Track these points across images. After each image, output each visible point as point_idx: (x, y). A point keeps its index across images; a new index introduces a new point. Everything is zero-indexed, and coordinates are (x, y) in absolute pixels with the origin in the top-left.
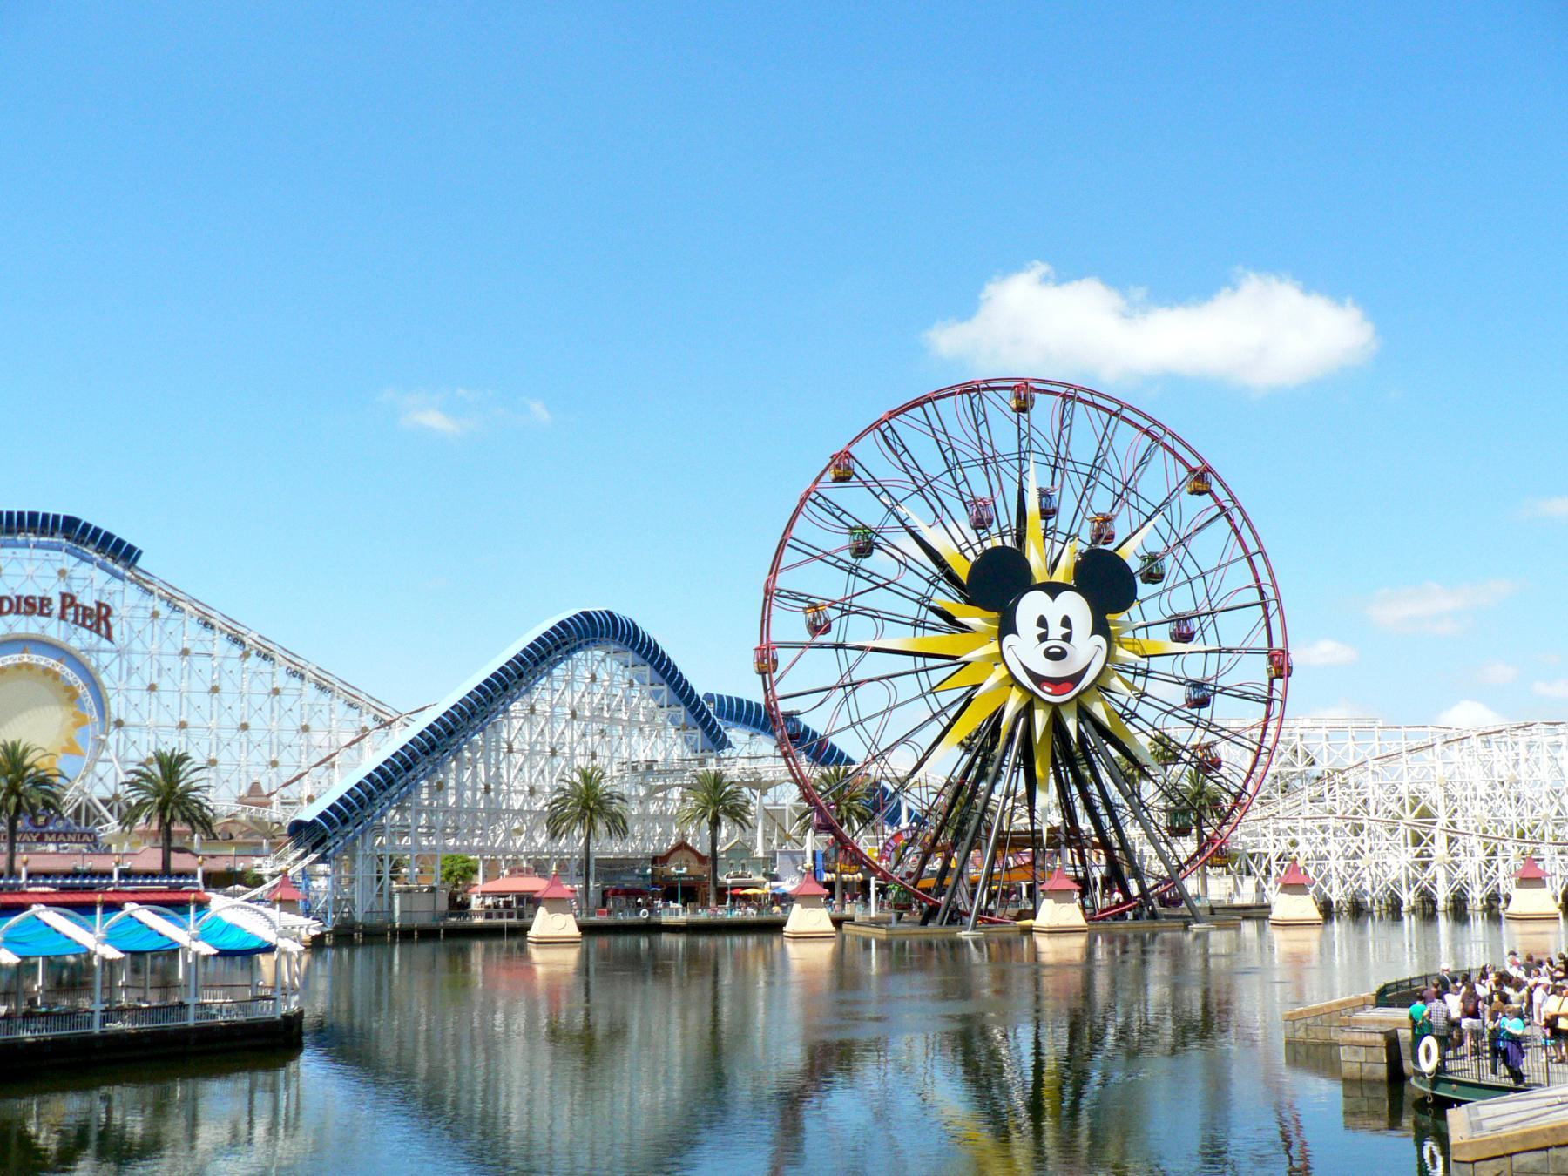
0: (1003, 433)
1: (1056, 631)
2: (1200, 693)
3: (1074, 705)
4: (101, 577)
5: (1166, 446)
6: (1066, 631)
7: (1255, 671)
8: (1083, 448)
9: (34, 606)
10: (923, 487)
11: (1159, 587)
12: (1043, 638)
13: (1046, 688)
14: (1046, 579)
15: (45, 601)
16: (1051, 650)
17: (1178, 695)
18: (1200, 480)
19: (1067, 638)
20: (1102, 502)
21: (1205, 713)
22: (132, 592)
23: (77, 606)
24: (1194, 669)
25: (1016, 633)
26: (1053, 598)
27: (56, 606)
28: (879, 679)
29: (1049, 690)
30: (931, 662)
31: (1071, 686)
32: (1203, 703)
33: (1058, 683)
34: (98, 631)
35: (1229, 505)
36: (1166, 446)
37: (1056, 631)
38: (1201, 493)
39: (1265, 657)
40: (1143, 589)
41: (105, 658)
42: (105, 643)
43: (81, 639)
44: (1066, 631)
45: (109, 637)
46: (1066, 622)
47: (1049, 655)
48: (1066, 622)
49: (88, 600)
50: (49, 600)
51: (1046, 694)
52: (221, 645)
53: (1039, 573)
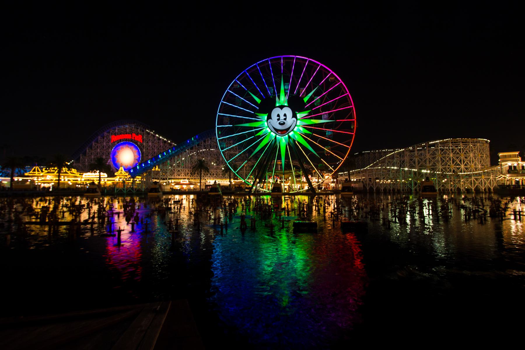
1: (282, 117)
3: (287, 136)
6: (285, 117)
12: (278, 120)
13: (279, 132)
16: (281, 123)
19: (285, 119)
25: (271, 118)
26: (282, 110)
29: (280, 133)
37: (282, 117)
44: (285, 117)
47: (280, 124)
48: (285, 115)
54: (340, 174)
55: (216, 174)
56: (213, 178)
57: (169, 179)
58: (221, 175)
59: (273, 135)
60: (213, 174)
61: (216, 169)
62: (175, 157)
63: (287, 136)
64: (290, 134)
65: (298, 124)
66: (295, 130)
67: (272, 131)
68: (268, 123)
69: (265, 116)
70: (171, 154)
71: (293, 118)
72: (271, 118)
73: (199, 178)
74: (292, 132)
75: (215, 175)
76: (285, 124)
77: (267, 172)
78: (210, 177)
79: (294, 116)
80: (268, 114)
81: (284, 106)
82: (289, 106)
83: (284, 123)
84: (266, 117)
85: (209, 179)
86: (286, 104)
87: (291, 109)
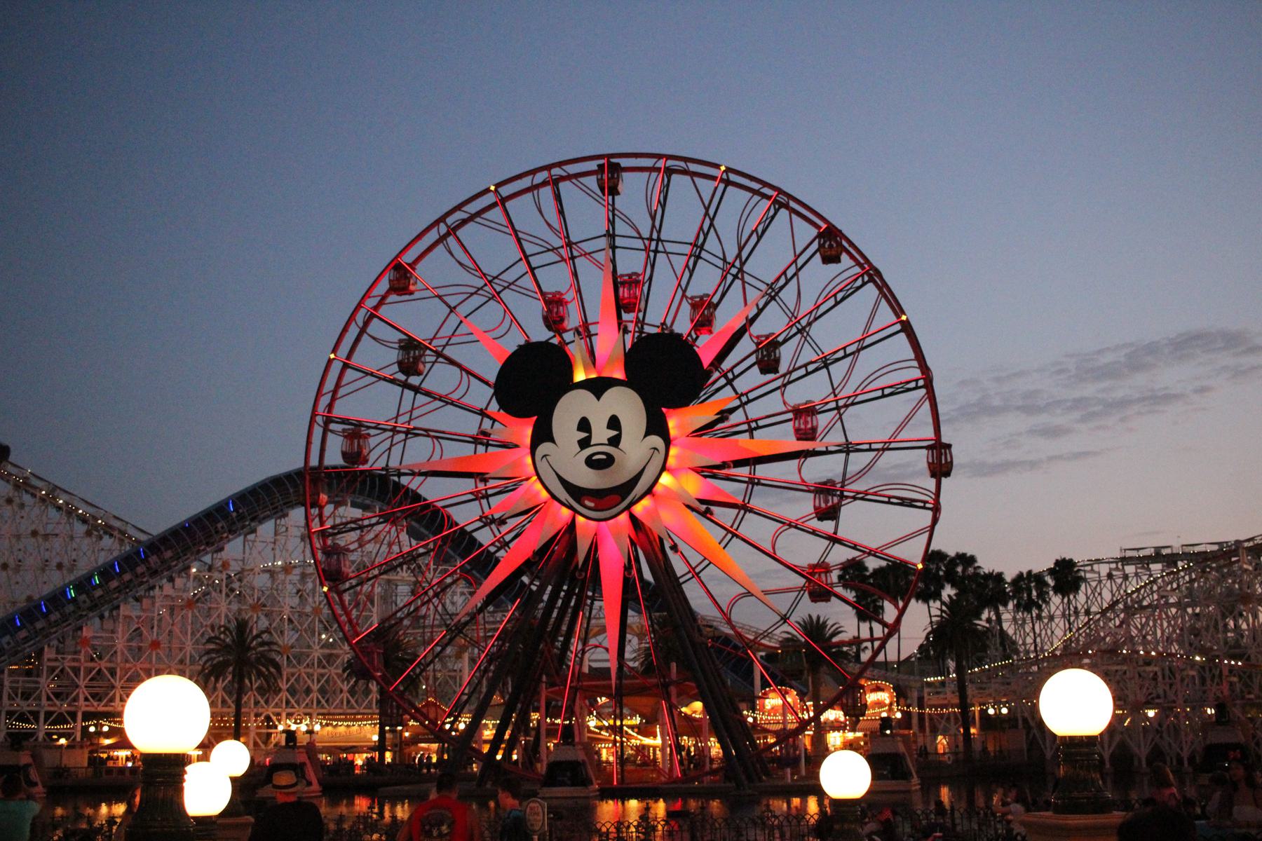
1: (601, 433)
3: (624, 517)
12: (584, 444)
13: (587, 503)
16: (594, 458)
17: (802, 507)
19: (615, 441)
20: (705, 280)
26: (598, 398)
29: (592, 505)
31: (619, 498)
37: (601, 433)
38: (837, 260)
44: (615, 433)
46: (614, 423)
47: (590, 462)
48: (614, 423)
52: (80, 528)
54: (929, 684)
55: (322, 691)
56: (302, 710)
57: (88, 716)
58: (345, 695)
59: (565, 512)
60: (308, 691)
61: (320, 661)
62: (118, 607)
63: (624, 517)
64: (638, 509)
65: (671, 461)
66: (658, 488)
67: (553, 496)
68: (538, 458)
69: (524, 431)
70: (98, 593)
71: (648, 438)
73: (232, 709)
74: (646, 502)
75: (315, 695)
76: (615, 464)
77: (544, 685)
78: (293, 707)
79: (656, 426)
80: (535, 418)
82: (631, 382)
83: (609, 461)
84: (529, 432)
85: (284, 715)
86: (619, 375)
87: (640, 395)
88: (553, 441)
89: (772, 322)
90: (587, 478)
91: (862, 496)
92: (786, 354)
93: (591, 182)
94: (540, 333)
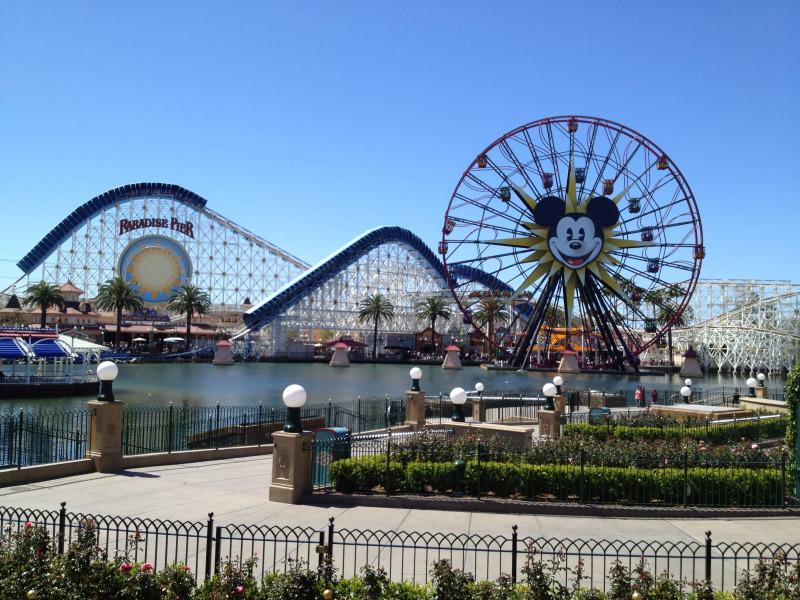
0: (561, 143)
1: (576, 235)
2: (654, 266)
4: (190, 211)
5: (646, 146)
7: (687, 255)
8: (601, 148)
9: (159, 223)
10: (521, 169)
11: (638, 214)
12: (569, 239)
14: (572, 211)
15: (165, 221)
17: (643, 266)
18: (664, 162)
19: (582, 239)
21: (657, 275)
22: (204, 218)
23: (178, 224)
24: (653, 253)
26: (576, 220)
27: (169, 223)
28: (495, 257)
30: (518, 249)
32: (655, 270)
33: (575, 259)
34: (187, 234)
35: (677, 174)
36: (646, 146)
37: (576, 235)
38: (664, 169)
39: (692, 249)
40: (625, 215)
41: (192, 245)
42: (187, 238)
43: (180, 237)
45: (192, 236)
46: (582, 231)
47: (571, 246)
48: (582, 231)
49: (182, 220)
50: (167, 221)
51: (570, 264)
52: (242, 240)
53: (569, 208)
72: (556, 236)
79: (599, 233)
81: (581, 215)
87: (594, 221)
88: (556, 236)
89: (635, 193)
90: (570, 252)
91: (667, 264)
92: (643, 203)
93: (565, 125)
94: (543, 192)
